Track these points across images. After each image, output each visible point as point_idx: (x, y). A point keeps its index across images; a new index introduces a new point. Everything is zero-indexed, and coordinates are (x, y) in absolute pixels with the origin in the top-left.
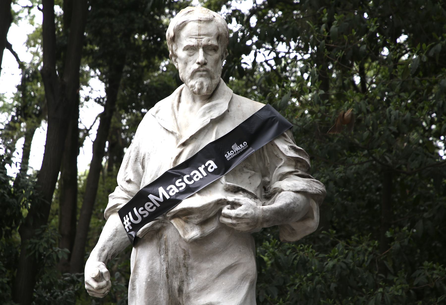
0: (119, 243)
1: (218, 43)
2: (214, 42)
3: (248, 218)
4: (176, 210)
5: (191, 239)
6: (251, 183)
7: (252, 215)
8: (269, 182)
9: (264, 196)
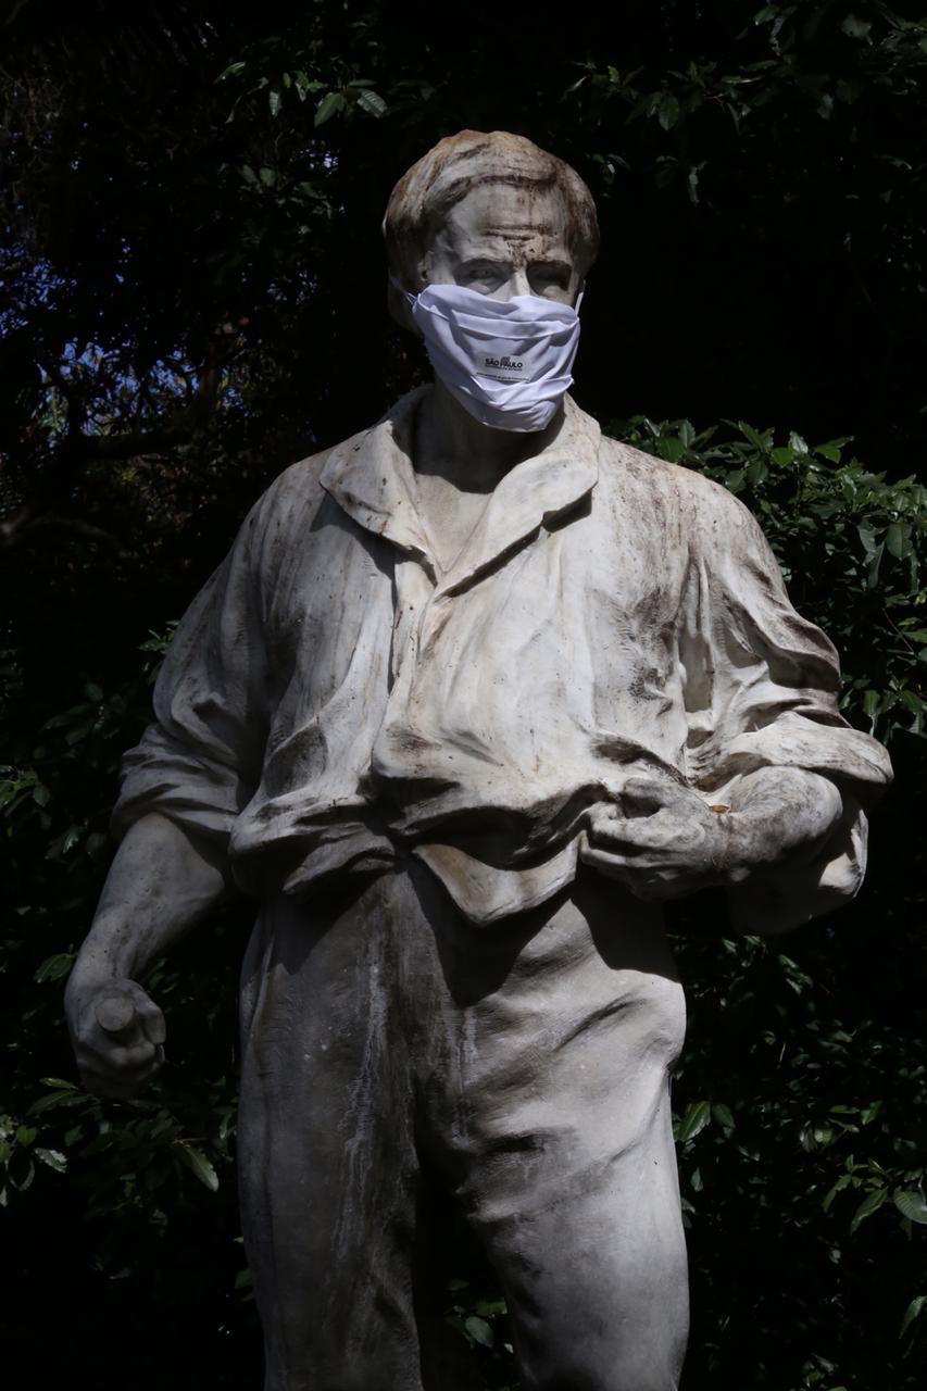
2: (560, 255)
3: (686, 853)
4: (440, 817)
5: (491, 914)
6: (663, 735)
7: (697, 842)
8: (710, 734)
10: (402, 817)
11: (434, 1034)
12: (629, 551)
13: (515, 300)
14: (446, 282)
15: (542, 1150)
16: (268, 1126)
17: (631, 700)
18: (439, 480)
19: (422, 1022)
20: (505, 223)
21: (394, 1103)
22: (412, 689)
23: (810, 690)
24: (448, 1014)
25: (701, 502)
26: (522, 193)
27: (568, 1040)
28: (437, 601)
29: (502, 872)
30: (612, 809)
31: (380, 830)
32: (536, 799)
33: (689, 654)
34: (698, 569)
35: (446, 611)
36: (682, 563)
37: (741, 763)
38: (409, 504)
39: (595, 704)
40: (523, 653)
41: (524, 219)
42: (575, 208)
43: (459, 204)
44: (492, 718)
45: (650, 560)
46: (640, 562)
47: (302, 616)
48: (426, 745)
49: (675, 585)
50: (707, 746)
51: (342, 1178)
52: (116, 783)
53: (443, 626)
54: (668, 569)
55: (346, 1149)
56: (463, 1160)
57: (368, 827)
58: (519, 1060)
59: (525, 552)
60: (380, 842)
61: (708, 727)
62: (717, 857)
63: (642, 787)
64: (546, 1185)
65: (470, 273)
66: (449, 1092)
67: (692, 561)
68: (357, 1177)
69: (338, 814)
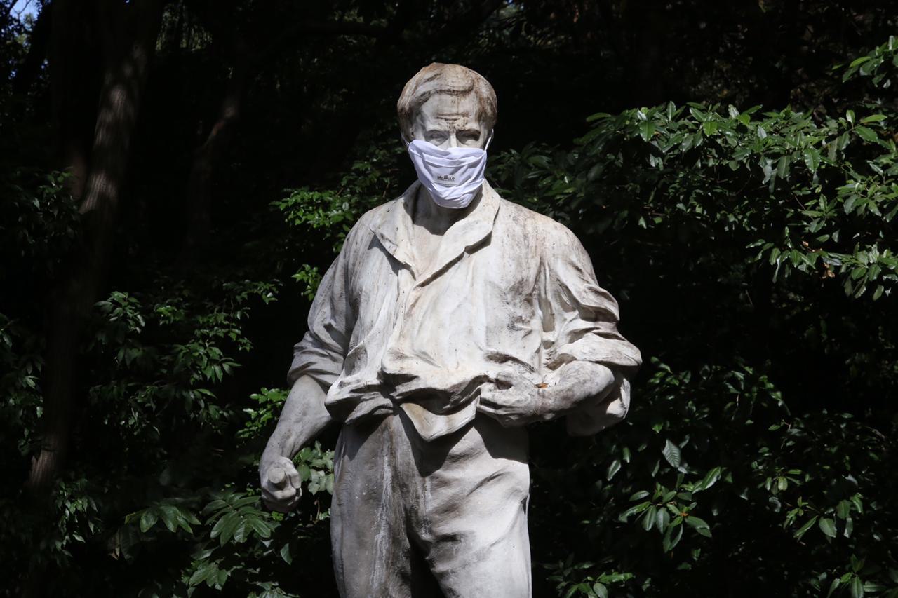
0: (313, 425)
1: (480, 126)
2: (473, 126)
3: (521, 407)
4: (410, 391)
7: (526, 403)
8: (553, 343)
9: (545, 364)
10: (395, 390)
11: (412, 488)
12: (508, 262)
13: (449, 150)
14: (421, 139)
15: (460, 541)
16: (342, 528)
17: (508, 332)
18: (423, 228)
19: (406, 483)
20: (445, 113)
21: (396, 519)
22: (401, 331)
23: (600, 322)
24: (418, 479)
25: (548, 235)
26: (454, 98)
27: (473, 491)
28: (414, 289)
29: (439, 416)
30: (491, 386)
31: (386, 396)
32: (452, 384)
33: (543, 305)
34: (544, 267)
35: (418, 294)
36: (536, 265)
37: (565, 358)
38: (407, 241)
39: (487, 336)
40: (453, 313)
41: (455, 111)
42: (482, 101)
43: (425, 104)
44: (436, 345)
45: (519, 265)
46: (513, 267)
47: (361, 291)
48: (406, 357)
49: (532, 276)
50: (552, 349)
51: (374, 552)
52: (291, 358)
53: (416, 301)
54: (528, 268)
55: (376, 539)
56: (426, 543)
57: (382, 394)
58: (450, 500)
59: (456, 264)
60: (387, 401)
61: (553, 340)
62: (537, 409)
63: (505, 376)
64: (461, 557)
65: (430, 136)
66: (419, 514)
67: (542, 263)
68: (381, 551)
69: (369, 388)
